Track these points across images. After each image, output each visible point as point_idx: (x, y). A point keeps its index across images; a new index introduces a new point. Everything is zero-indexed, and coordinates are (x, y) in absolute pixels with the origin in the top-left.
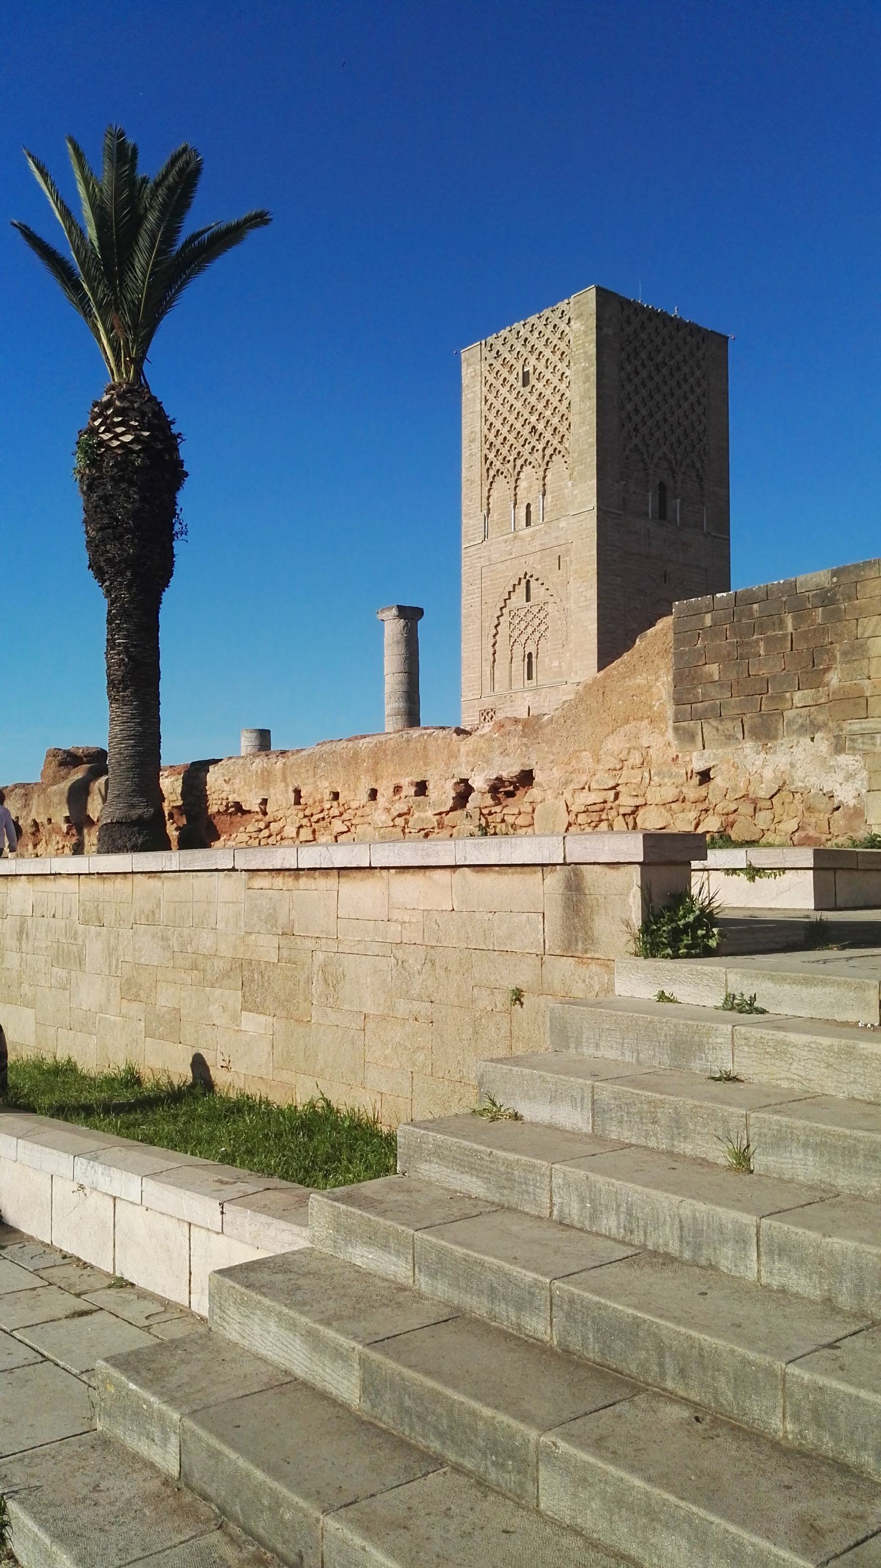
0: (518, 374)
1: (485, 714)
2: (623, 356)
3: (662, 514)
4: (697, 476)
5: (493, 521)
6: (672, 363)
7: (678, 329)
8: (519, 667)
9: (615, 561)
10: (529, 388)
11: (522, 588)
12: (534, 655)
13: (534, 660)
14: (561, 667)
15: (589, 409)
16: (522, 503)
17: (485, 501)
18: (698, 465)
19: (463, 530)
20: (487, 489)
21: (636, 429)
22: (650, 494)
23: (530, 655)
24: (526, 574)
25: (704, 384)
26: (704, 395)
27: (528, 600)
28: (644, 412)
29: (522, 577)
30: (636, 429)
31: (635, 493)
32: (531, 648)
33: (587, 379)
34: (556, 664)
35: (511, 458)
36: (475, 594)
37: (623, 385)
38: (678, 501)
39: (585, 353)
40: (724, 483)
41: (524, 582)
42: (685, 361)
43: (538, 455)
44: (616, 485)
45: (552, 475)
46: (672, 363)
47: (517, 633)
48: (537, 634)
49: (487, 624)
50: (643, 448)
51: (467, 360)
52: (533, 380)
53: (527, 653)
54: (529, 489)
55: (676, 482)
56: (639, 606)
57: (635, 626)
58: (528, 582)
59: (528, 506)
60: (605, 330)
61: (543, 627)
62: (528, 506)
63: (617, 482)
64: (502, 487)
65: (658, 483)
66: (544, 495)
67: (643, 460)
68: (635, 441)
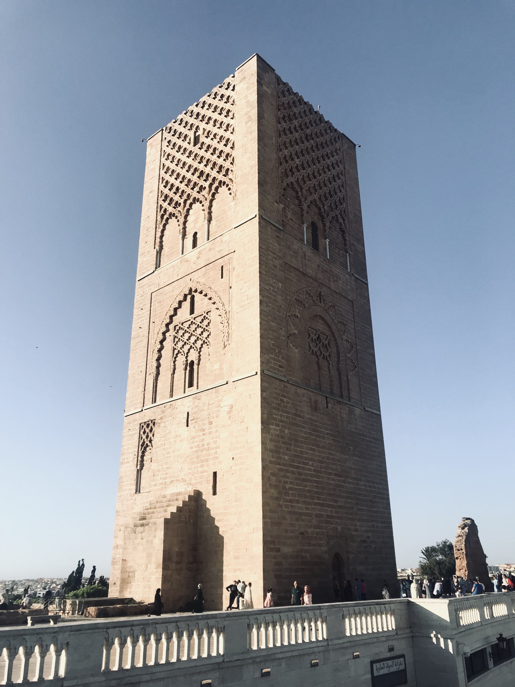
0: (190, 139)
1: (145, 427)
3: (315, 245)
4: (341, 229)
5: (164, 255)
8: (181, 375)
9: (276, 267)
10: (199, 145)
11: (186, 305)
12: (196, 362)
13: (195, 367)
14: (221, 369)
15: (251, 140)
16: (190, 233)
17: (158, 240)
18: (341, 220)
19: (139, 266)
20: (160, 230)
22: (305, 226)
23: (192, 363)
24: (191, 290)
27: (192, 312)
28: (297, 161)
29: (187, 292)
31: (292, 220)
32: (193, 356)
33: (250, 119)
34: (217, 366)
35: (182, 201)
36: (144, 316)
37: (280, 134)
38: (327, 241)
39: (248, 102)
40: (361, 240)
41: (189, 297)
43: (205, 192)
44: (276, 204)
45: (217, 203)
47: (180, 344)
48: (200, 343)
49: (153, 341)
51: (151, 144)
52: (202, 139)
53: (189, 362)
54: (196, 221)
55: (324, 226)
56: (299, 315)
57: (296, 332)
58: (193, 298)
59: (196, 233)
60: (265, 88)
61: (205, 334)
62: (196, 233)
63: (277, 202)
64: (174, 227)
66: (210, 220)
67: (297, 197)
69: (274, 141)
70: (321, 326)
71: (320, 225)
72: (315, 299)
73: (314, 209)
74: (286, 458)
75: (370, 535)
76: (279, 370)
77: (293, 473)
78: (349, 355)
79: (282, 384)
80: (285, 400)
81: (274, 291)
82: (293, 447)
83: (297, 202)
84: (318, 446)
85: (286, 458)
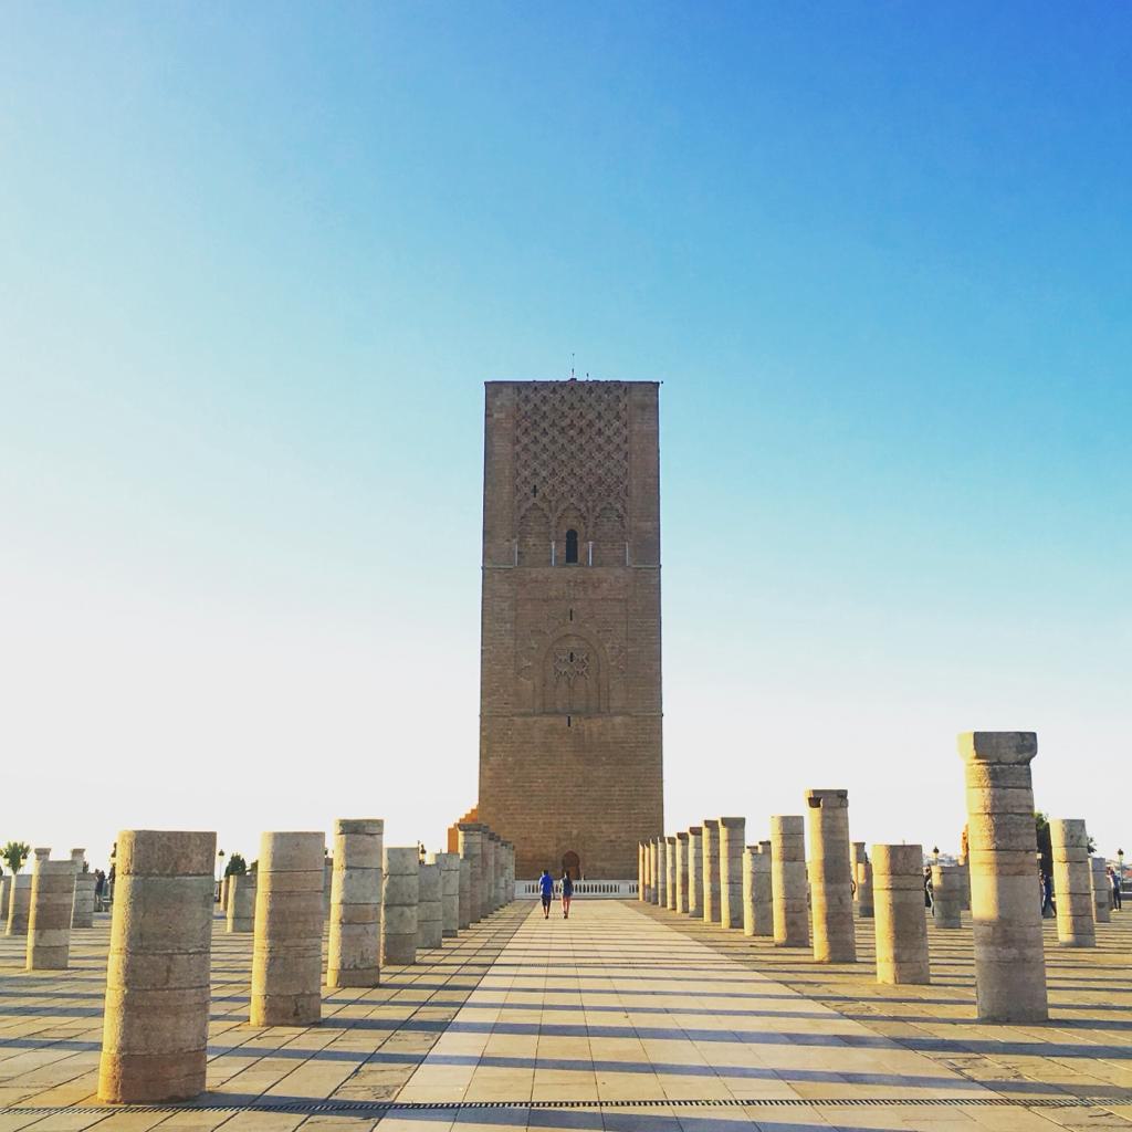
2: (518, 432)
3: (572, 556)
6: (583, 423)
7: (590, 391)
9: (503, 610)
18: (618, 506)
21: (535, 490)
25: (625, 432)
26: (626, 442)
30: (535, 490)
42: (599, 416)
44: (507, 543)
46: (583, 423)
50: (544, 506)
56: (536, 646)
63: (508, 540)
65: (565, 531)
67: (545, 516)
68: (533, 500)
69: (507, 471)
70: (573, 644)
71: (581, 530)
72: (561, 620)
73: (574, 513)
74: (508, 781)
75: (622, 835)
76: (502, 708)
77: (516, 792)
78: (613, 664)
79: (506, 719)
80: (510, 732)
81: (500, 635)
82: (516, 771)
83: (544, 520)
84: (550, 765)
85: (508, 781)
